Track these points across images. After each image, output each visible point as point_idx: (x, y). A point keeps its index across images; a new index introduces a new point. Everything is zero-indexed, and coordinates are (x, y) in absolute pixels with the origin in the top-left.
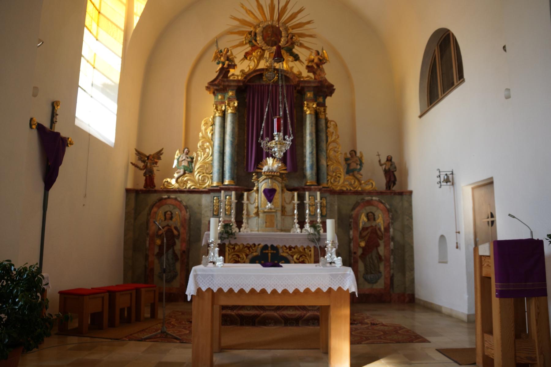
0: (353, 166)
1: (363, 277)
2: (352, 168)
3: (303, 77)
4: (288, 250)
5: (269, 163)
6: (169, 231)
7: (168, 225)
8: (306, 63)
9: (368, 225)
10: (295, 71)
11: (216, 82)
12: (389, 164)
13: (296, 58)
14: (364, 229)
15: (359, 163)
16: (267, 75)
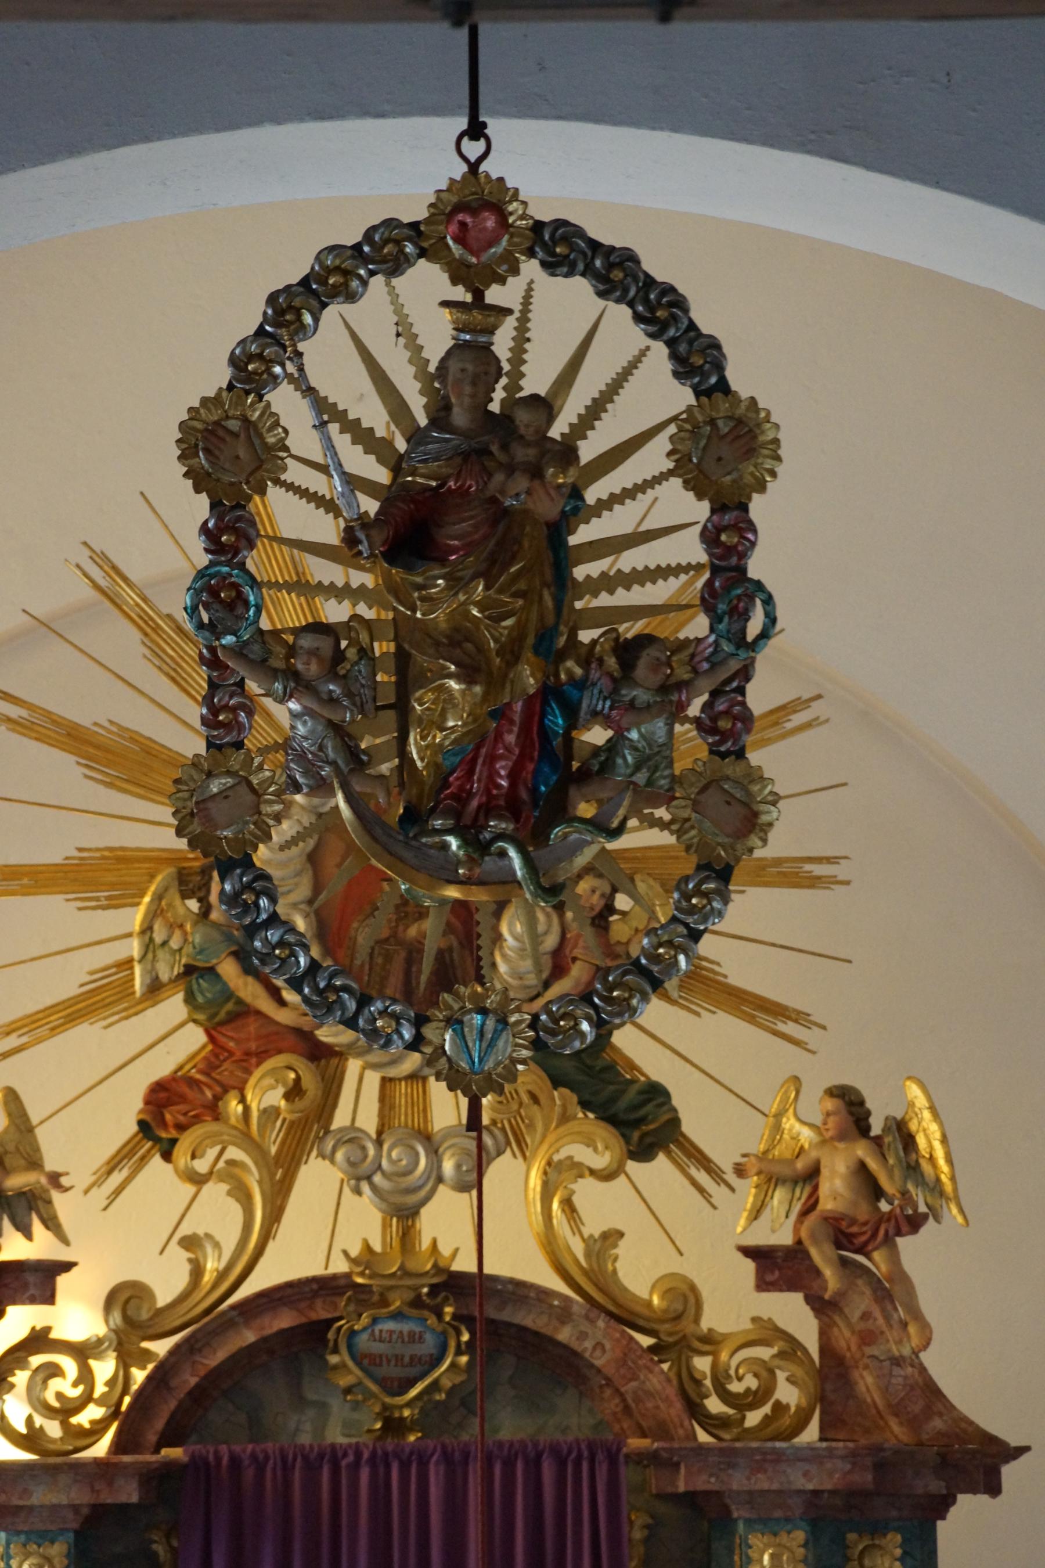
3: (711, 1341)
10: (639, 1274)
13: (642, 1121)
16: (363, 1341)
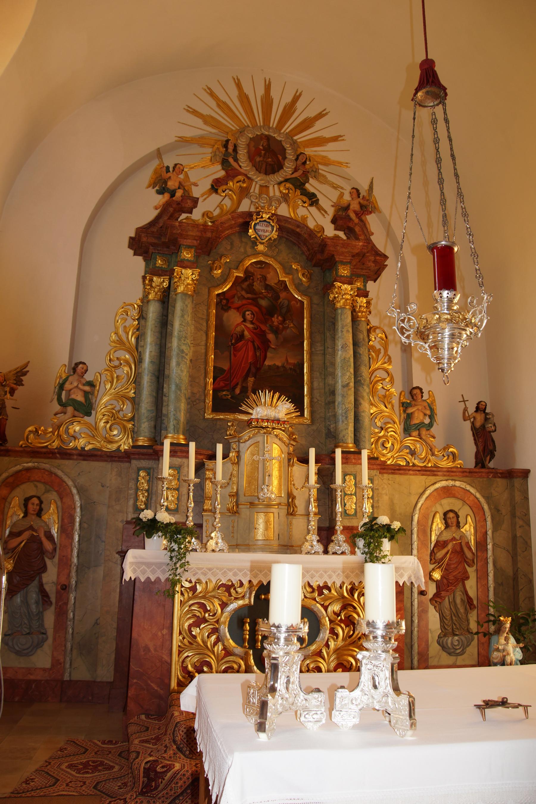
0: (418, 418)
1: (438, 643)
2: (416, 421)
4: (316, 594)
5: (263, 400)
6: (34, 540)
7: (31, 528)
8: (331, 211)
9: (447, 536)
10: (311, 224)
11: (154, 229)
12: (480, 418)
14: (440, 544)
15: (428, 412)
